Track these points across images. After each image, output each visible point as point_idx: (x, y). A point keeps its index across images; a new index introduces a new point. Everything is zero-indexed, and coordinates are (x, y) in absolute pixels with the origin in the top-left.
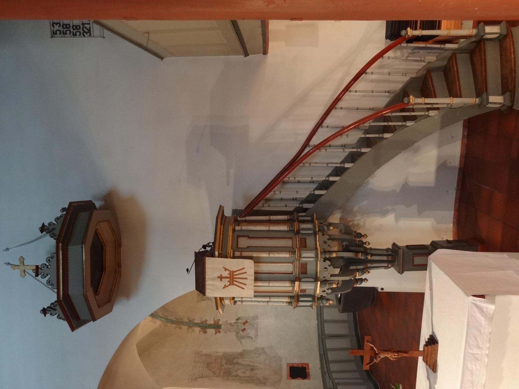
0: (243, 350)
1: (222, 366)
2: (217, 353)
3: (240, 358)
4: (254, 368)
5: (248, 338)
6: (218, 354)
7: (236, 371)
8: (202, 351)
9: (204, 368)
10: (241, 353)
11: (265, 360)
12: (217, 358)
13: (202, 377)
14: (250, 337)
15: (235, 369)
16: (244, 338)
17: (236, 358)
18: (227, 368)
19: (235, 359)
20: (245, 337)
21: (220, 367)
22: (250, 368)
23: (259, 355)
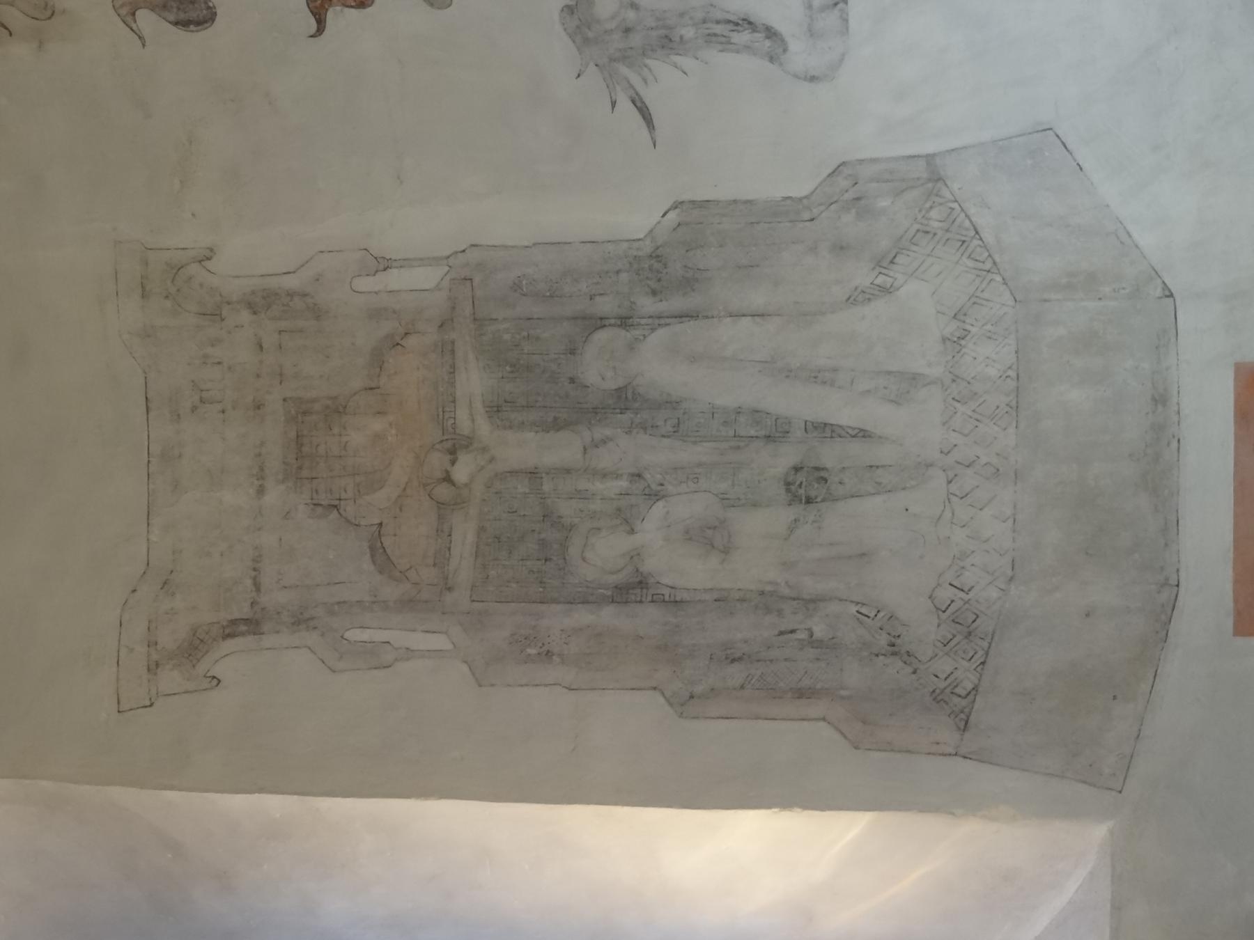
0: (675, 206)
1: (455, 447)
2: (385, 265)
3: (659, 320)
4: (830, 455)
5: (726, 44)
6: (395, 279)
7: (626, 520)
8: (207, 256)
9: (261, 491)
10: (656, 256)
11: (955, 342)
12: (395, 343)
13: (251, 625)
14: (748, 23)
15: (613, 487)
16: (668, 43)
17: (600, 323)
18: (513, 473)
19: (602, 336)
20: (689, 33)
21: (437, 461)
22: (783, 459)
23: (884, 262)
